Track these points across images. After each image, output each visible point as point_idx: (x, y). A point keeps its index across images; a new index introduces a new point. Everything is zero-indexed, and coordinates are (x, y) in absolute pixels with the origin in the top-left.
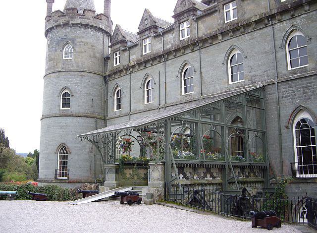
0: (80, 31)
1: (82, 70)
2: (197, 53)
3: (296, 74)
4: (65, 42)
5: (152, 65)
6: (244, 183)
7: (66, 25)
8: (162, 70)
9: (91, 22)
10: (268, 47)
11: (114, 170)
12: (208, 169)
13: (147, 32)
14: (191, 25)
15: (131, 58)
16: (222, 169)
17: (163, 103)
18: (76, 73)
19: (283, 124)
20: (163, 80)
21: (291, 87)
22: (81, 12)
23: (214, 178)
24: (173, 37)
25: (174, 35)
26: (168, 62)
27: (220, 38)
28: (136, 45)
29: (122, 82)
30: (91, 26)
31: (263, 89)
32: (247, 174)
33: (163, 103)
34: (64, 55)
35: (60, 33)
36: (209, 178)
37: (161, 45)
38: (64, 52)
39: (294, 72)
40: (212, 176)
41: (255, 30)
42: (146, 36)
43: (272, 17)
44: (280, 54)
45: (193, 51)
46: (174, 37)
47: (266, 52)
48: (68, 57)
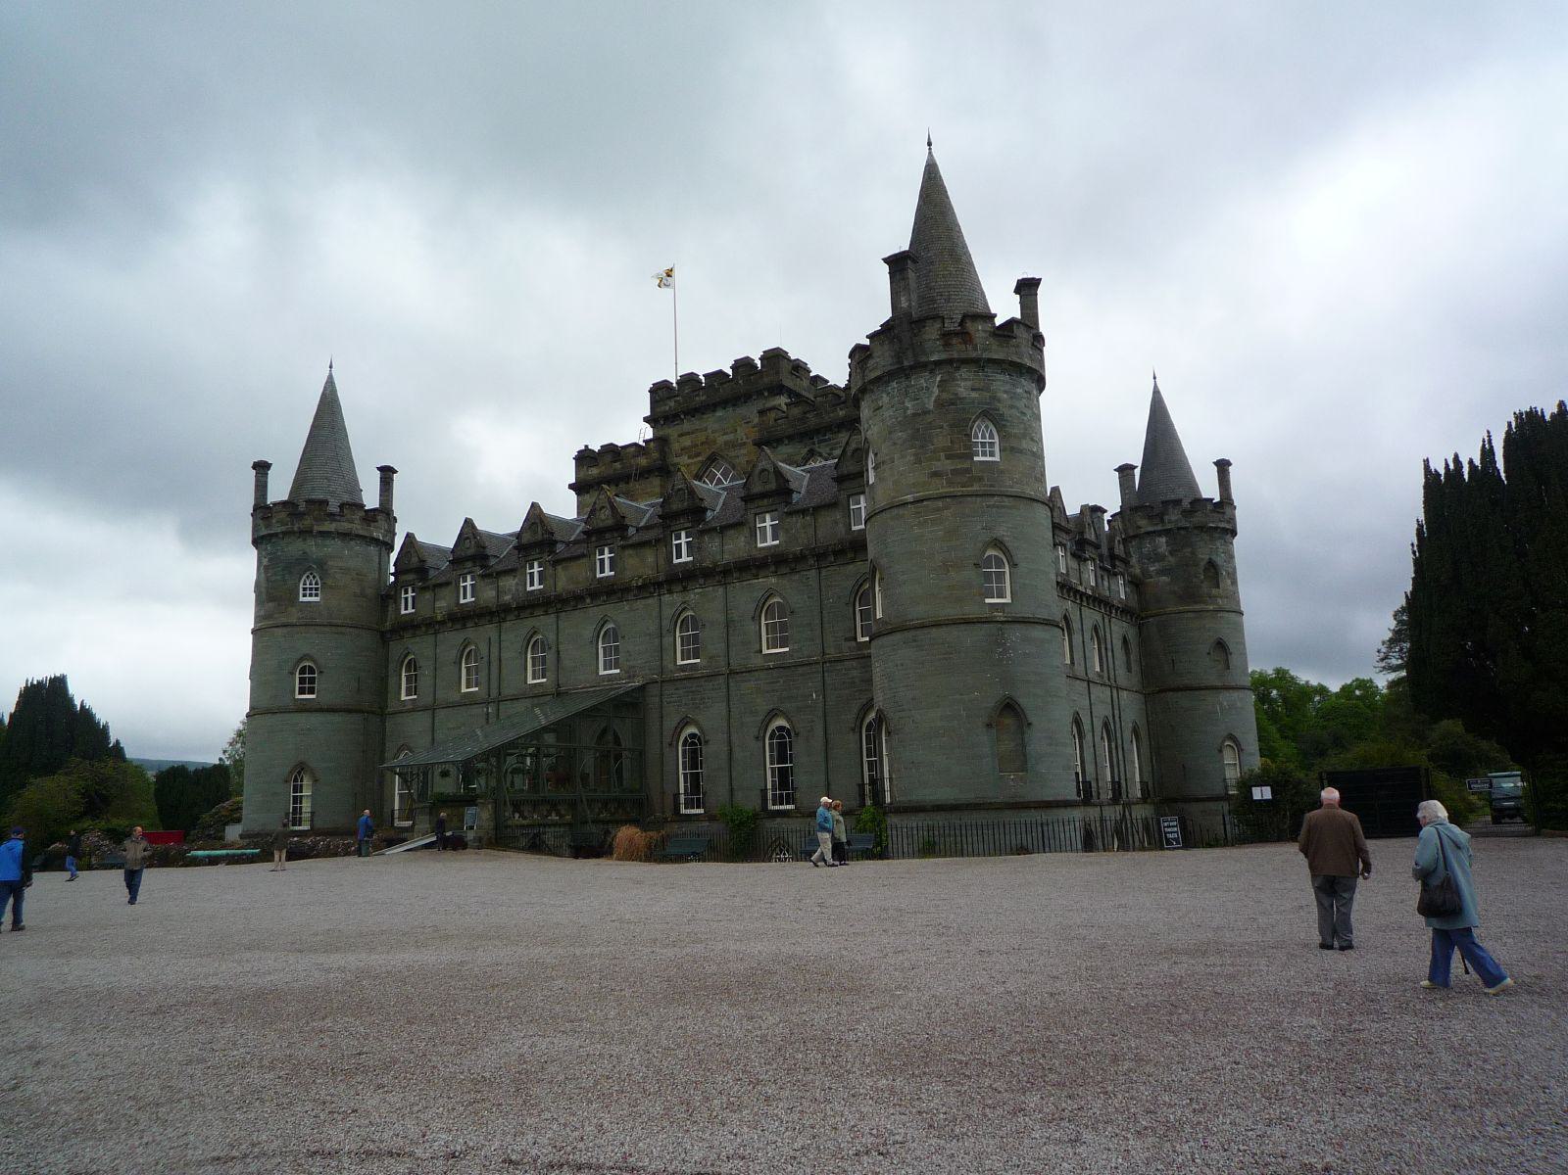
0: (333, 547)
1: (340, 622)
2: (552, 618)
3: (685, 671)
4: (302, 565)
5: (476, 625)
6: (608, 822)
7: (305, 533)
8: (494, 636)
9: (357, 527)
11: (427, 810)
12: (554, 806)
13: (469, 564)
14: (545, 569)
15: (438, 604)
16: (573, 805)
18: (327, 629)
19: (667, 740)
21: (677, 689)
22: (333, 507)
23: (561, 816)
24: (514, 582)
25: (516, 580)
26: (507, 625)
27: (588, 601)
28: (447, 584)
29: (420, 647)
30: (359, 536)
31: (642, 688)
32: (613, 810)
33: (494, 693)
34: (301, 592)
35: (294, 548)
36: (554, 817)
37: (493, 593)
38: (301, 586)
39: (683, 668)
40: (558, 814)
42: (465, 571)
43: (659, 585)
44: (668, 640)
46: (517, 584)
47: (650, 635)
48: (311, 595)
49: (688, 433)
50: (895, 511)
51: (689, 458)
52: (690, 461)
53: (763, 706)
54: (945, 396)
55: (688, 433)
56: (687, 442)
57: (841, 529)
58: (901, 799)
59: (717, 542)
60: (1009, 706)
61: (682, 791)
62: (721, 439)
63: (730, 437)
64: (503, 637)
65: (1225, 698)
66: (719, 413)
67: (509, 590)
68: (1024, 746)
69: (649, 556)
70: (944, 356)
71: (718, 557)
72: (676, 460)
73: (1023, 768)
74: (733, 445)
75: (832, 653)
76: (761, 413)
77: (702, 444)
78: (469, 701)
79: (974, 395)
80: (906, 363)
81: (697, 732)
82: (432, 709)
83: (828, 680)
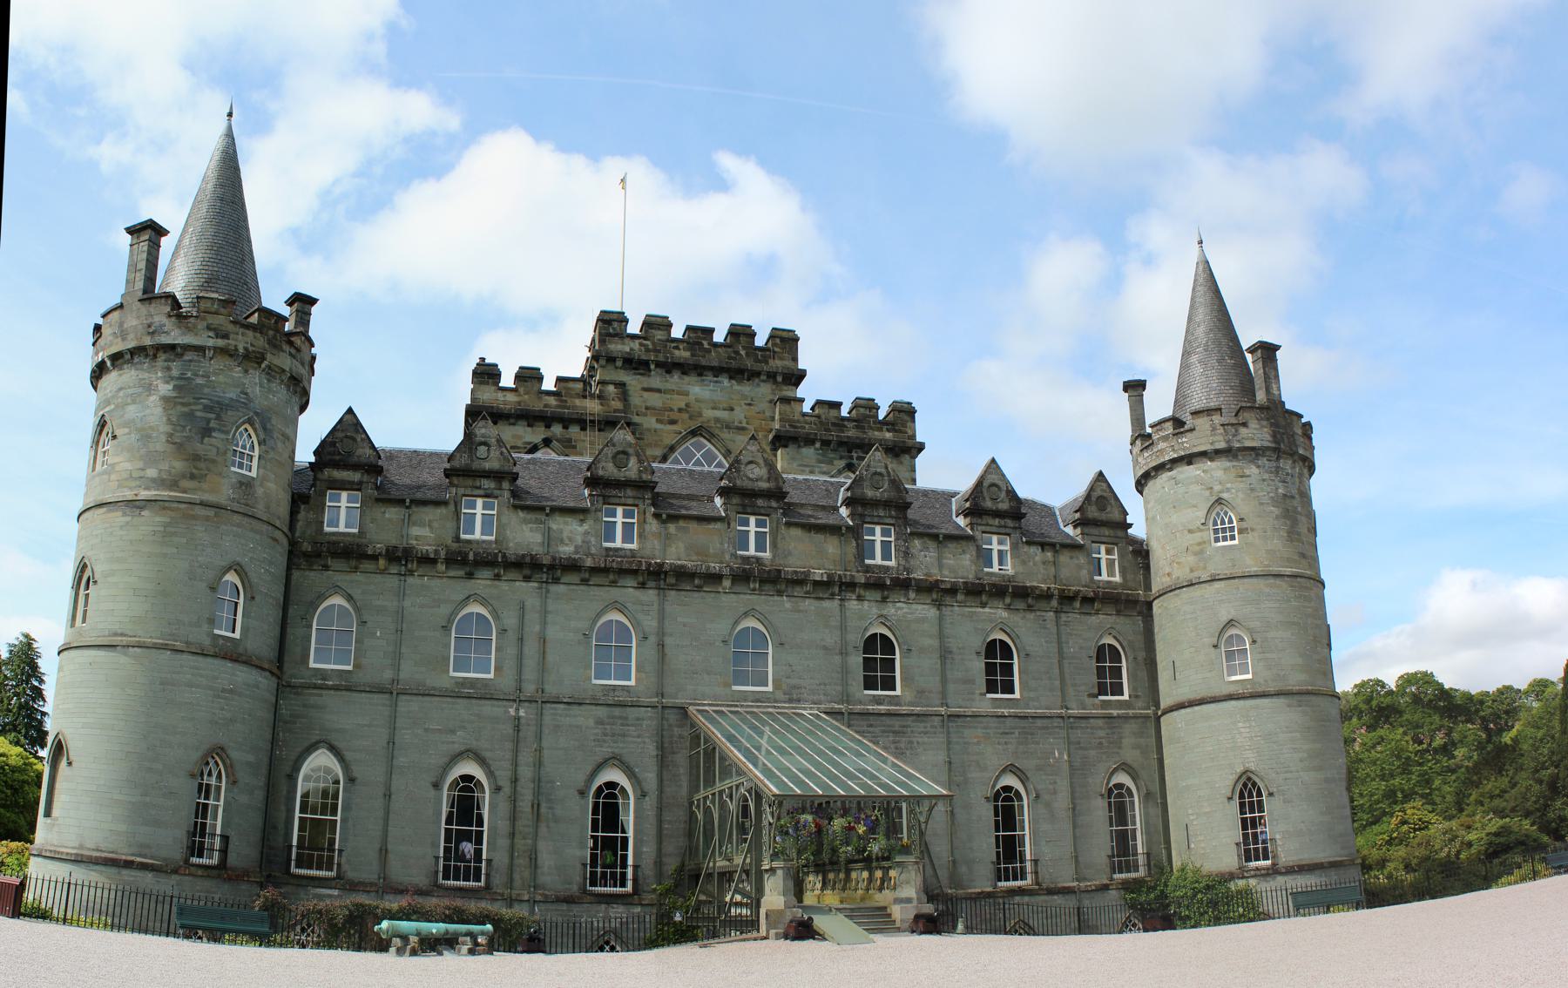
10: (831, 638)
18: (265, 527)
20: (533, 628)
25: (586, 527)
41: (808, 595)
46: (587, 533)
47: (825, 648)
49: (659, 391)
52: (659, 426)
55: (659, 391)
56: (655, 400)
61: (295, 843)
63: (719, 414)
67: (570, 539)
69: (832, 546)
77: (680, 410)
82: (391, 691)
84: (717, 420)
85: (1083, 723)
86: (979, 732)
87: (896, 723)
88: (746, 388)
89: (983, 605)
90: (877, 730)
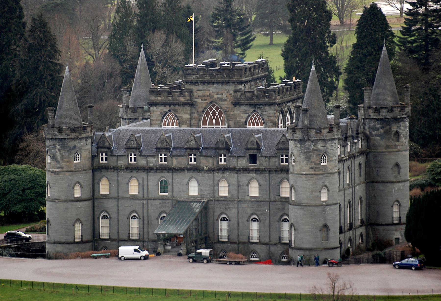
10: (211, 183)
17: (145, 196)
19: (215, 219)
26: (149, 174)
33: (145, 196)
37: (145, 162)
45: (168, 172)
47: (209, 185)
49: (201, 90)
50: (300, 175)
51: (202, 100)
52: (202, 102)
53: (249, 212)
54: (315, 148)
55: (201, 90)
56: (200, 93)
57: (277, 164)
58: (297, 246)
59: (235, 160)
60: (326, 226)
62: (216, 96)
63: (220, 96)
64: (149, 178)
65: (396, 186)
66: (215, 86)
68: (328, 234)
69: (210, 160)
70: (315, 139)
71: (236, 165)
72: (196, 100)
73: (327, 240)
74: (221, 100)
75: (273, 199)
76: (235, 91)
77: (208, 96)
78: (134, 197)
79: (322, 148)
80: (306, 139)
81: (226, 217)
83: (271, 207)
84: (218, 98)
85: (274, 203)
86: (246, 205)
87: (226, 203)
88: (226, 87)
89: (249, 173)
90: (221, 204)
